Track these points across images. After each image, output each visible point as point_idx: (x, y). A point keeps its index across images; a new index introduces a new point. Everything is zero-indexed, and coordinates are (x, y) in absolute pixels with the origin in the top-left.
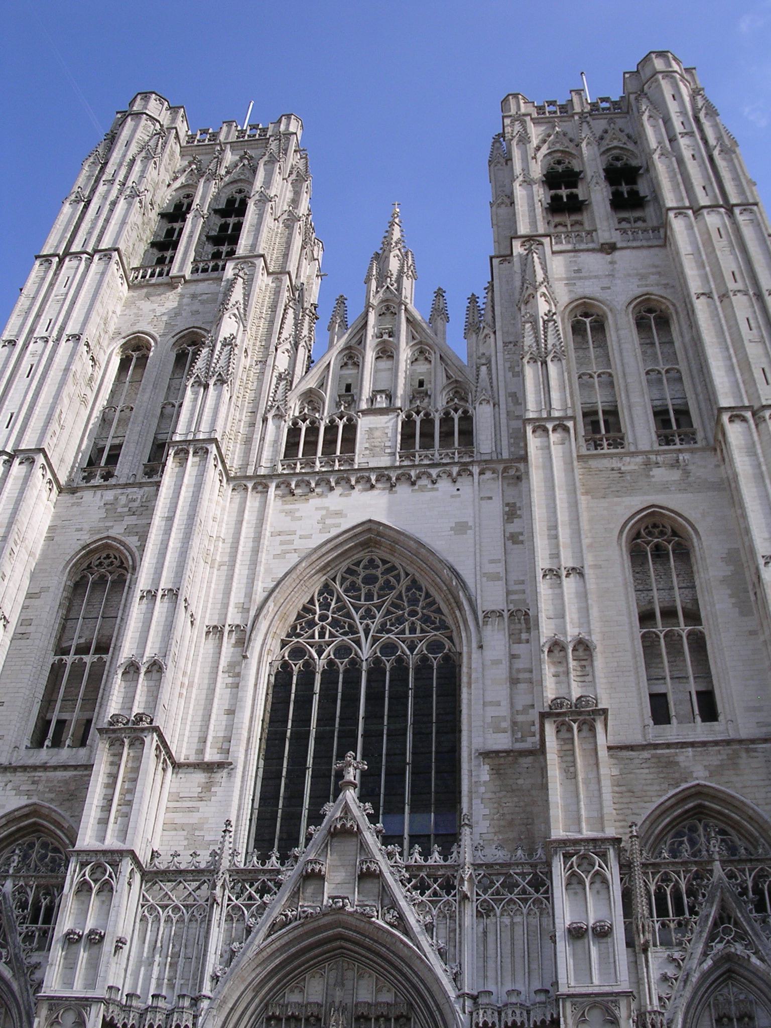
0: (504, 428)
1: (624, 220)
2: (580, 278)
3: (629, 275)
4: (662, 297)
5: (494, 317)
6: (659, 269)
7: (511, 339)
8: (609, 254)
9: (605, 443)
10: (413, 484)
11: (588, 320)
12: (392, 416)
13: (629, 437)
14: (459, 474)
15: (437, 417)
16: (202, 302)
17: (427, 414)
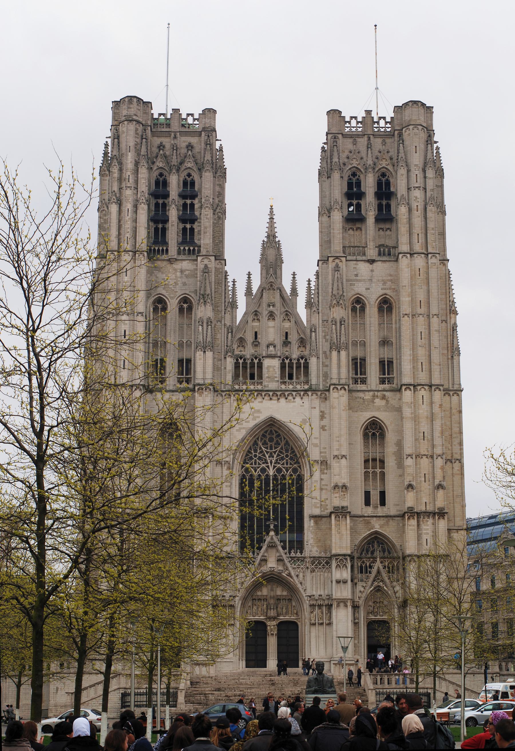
0: (321, 372)
1: (381, 229)
2: (357, 281)
3: (379, 281)
6: (392, 278)
7: (325, 318)
10: (286, 399)
11: (358, 306)
12: (277, 359)
13: (368, 381)
14: (304, 395)
15: (295, 362)
16: (187, 276)
17: (291, 360)
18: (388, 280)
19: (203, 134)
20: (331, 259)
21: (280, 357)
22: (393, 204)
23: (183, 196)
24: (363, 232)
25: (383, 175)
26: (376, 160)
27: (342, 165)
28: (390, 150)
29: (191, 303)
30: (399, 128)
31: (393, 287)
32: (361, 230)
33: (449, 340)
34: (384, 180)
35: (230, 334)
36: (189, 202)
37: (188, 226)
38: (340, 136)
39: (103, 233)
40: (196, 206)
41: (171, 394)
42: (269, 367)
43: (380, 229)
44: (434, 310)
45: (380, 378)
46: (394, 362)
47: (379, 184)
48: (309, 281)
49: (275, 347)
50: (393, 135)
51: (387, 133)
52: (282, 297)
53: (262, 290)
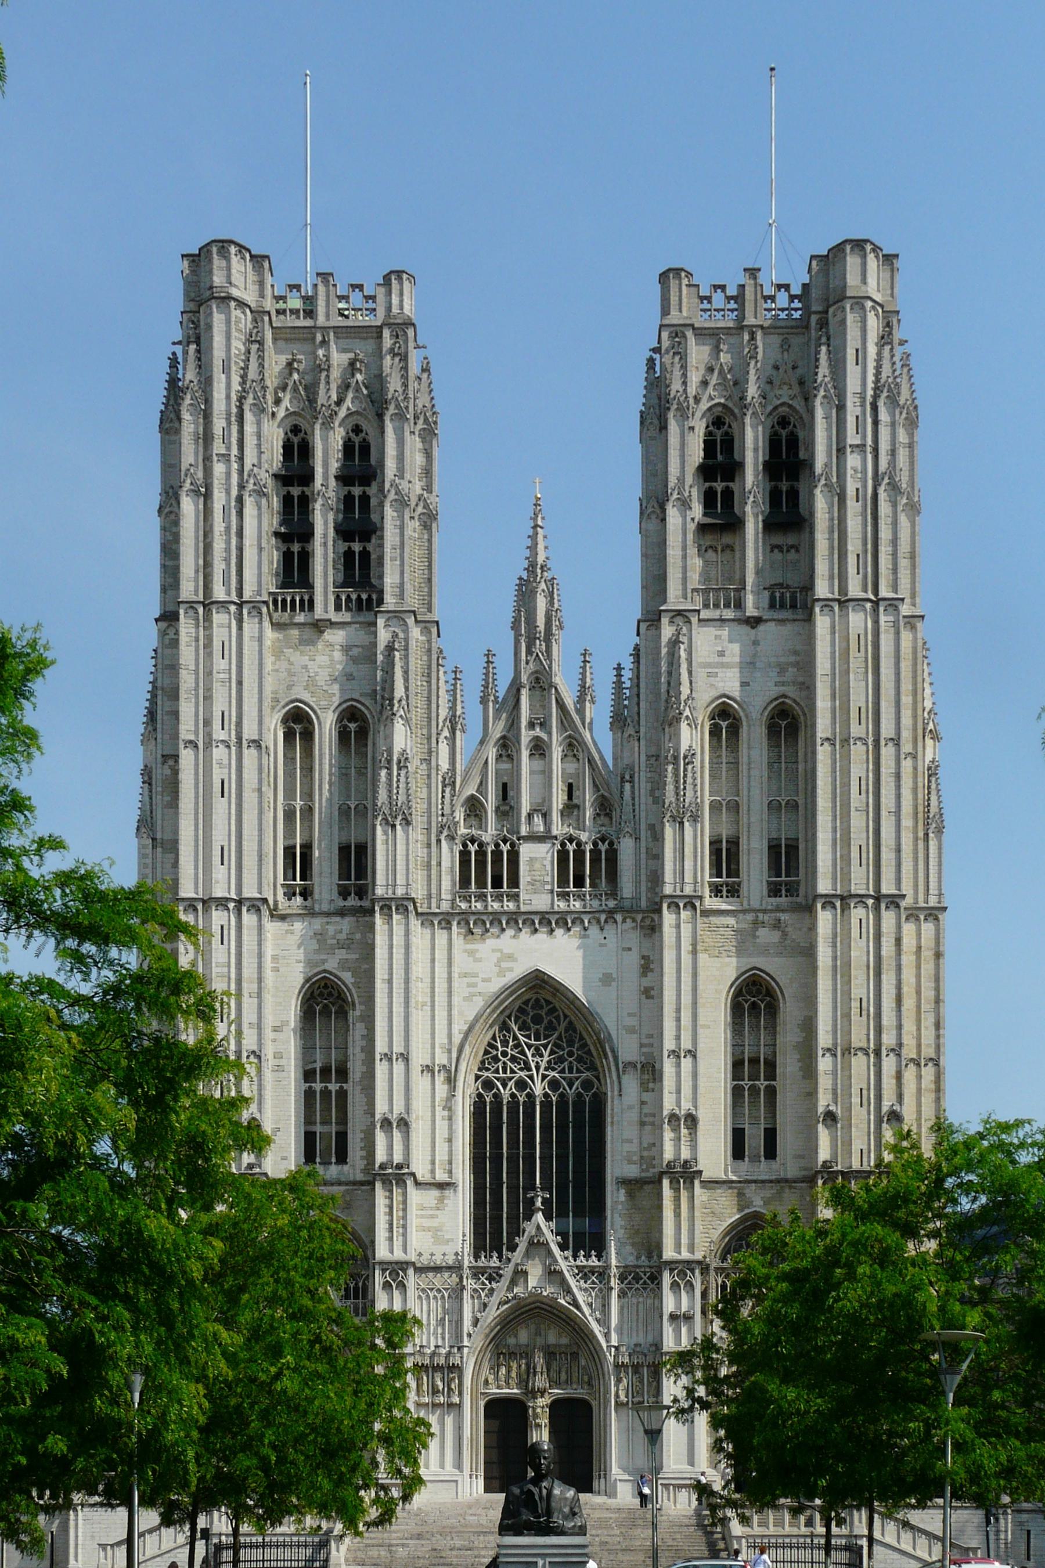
0: (643, 871)
1: (779, 547)
4: (795, 701)
5: (639, 714)
7: (653, 750)
8: (753, 628)
9: (725, 889)
11: (724, 724)
13: (744, 891)
14: (606, 921)
17: (579, 844)
18: (788, 664)
19: (386, 333)
20: (665, 620)
21: (556, 838)
22: (802, 488)
23: (344, 479)
24: (738, 555)
25: (783, 422)
26: (768, 387)
27: (691, 401)
28: (800, 363)
29: (365, 720)
30: (820, 309)
31: (801, 679)
32: (733, 550)
33: (920, 796)
34: (784, 433)
35: (448, 790)
36: (357, 491)
37: (357, 547)
38: (689, 334)
39: (169, 563)
40: (373, 502)
41: (325, 920)
42: (532, 860)
43: (773, 548)
44: (887, 730)
45: (769, 883)
46: (801, 847)
47: (774, 444)
48: (619, 668)
49: (545, 815)
50: (807, 327)
51: (794, 323)
52: (561, 705)
53: (518, 691)
